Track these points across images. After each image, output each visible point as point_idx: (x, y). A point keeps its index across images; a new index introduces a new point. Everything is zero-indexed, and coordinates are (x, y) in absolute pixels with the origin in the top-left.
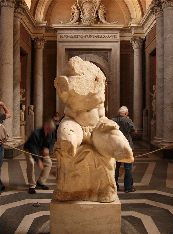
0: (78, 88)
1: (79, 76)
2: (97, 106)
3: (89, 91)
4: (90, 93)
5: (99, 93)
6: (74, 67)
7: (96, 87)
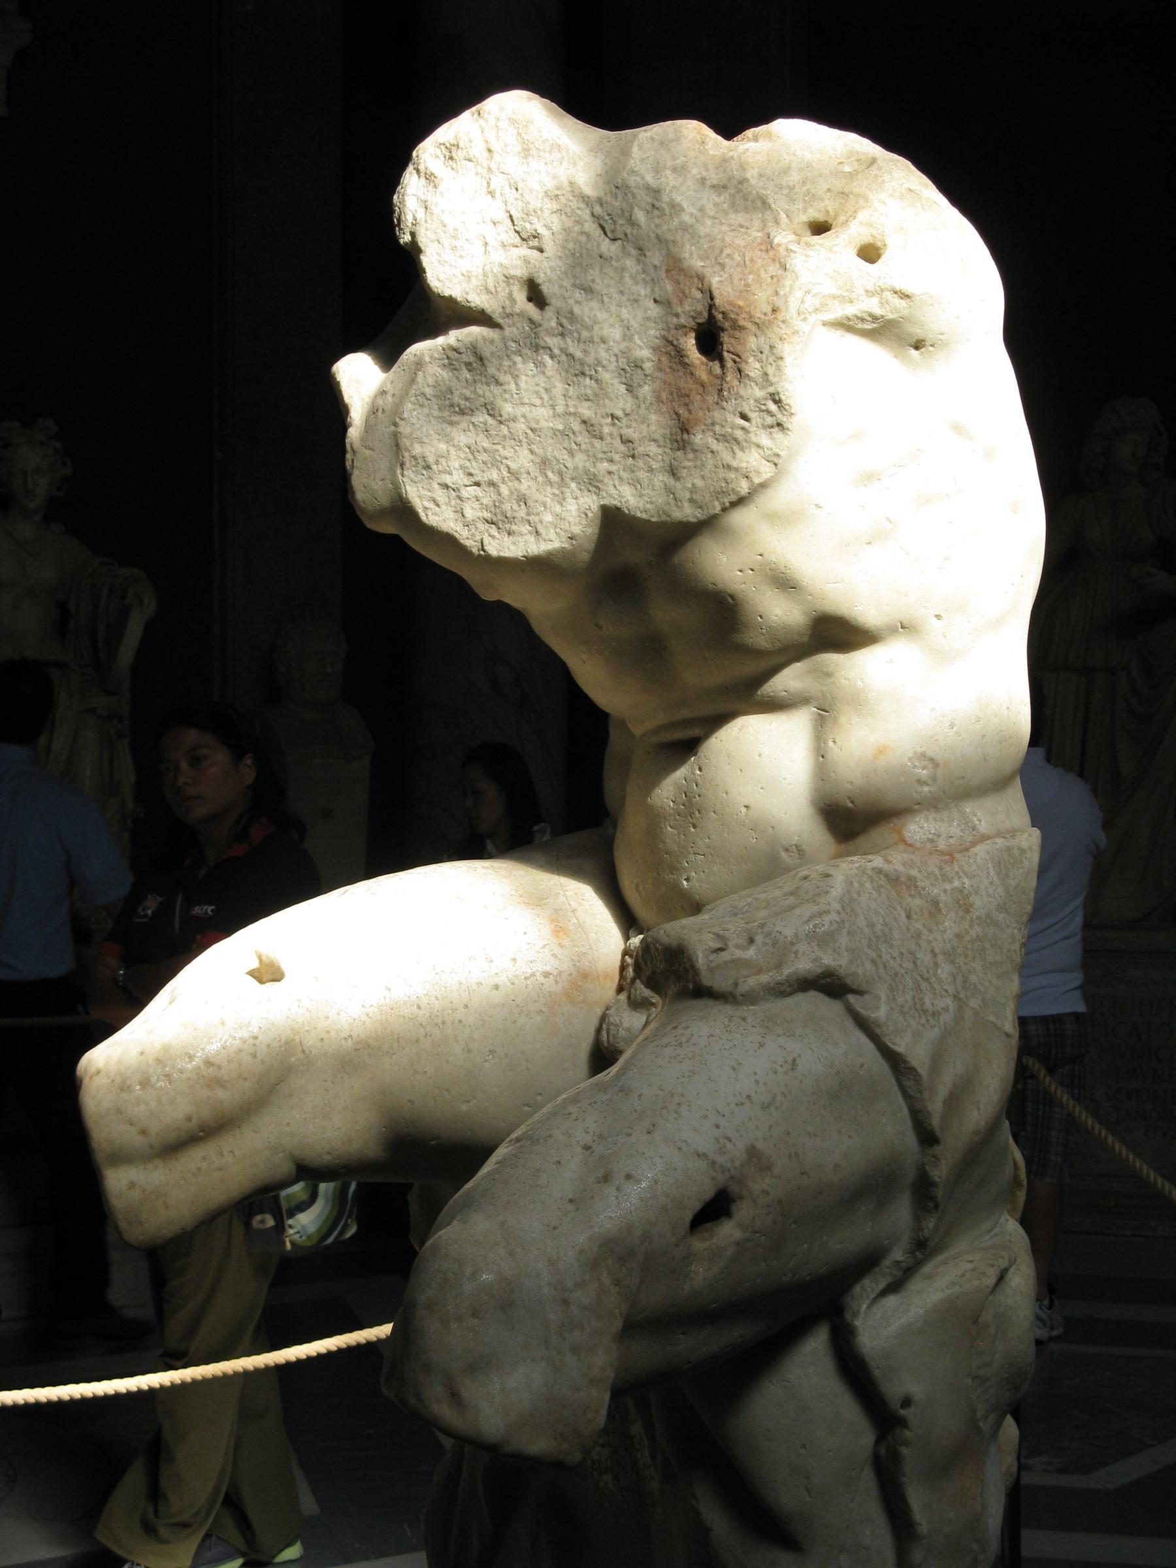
0: (456, 478)
1: (474, 332)
2: (789, 680)
3: (592, 503)
4: (612, 520)
5: (741, 518)
6: (422, 241)
7: (698, 439)
